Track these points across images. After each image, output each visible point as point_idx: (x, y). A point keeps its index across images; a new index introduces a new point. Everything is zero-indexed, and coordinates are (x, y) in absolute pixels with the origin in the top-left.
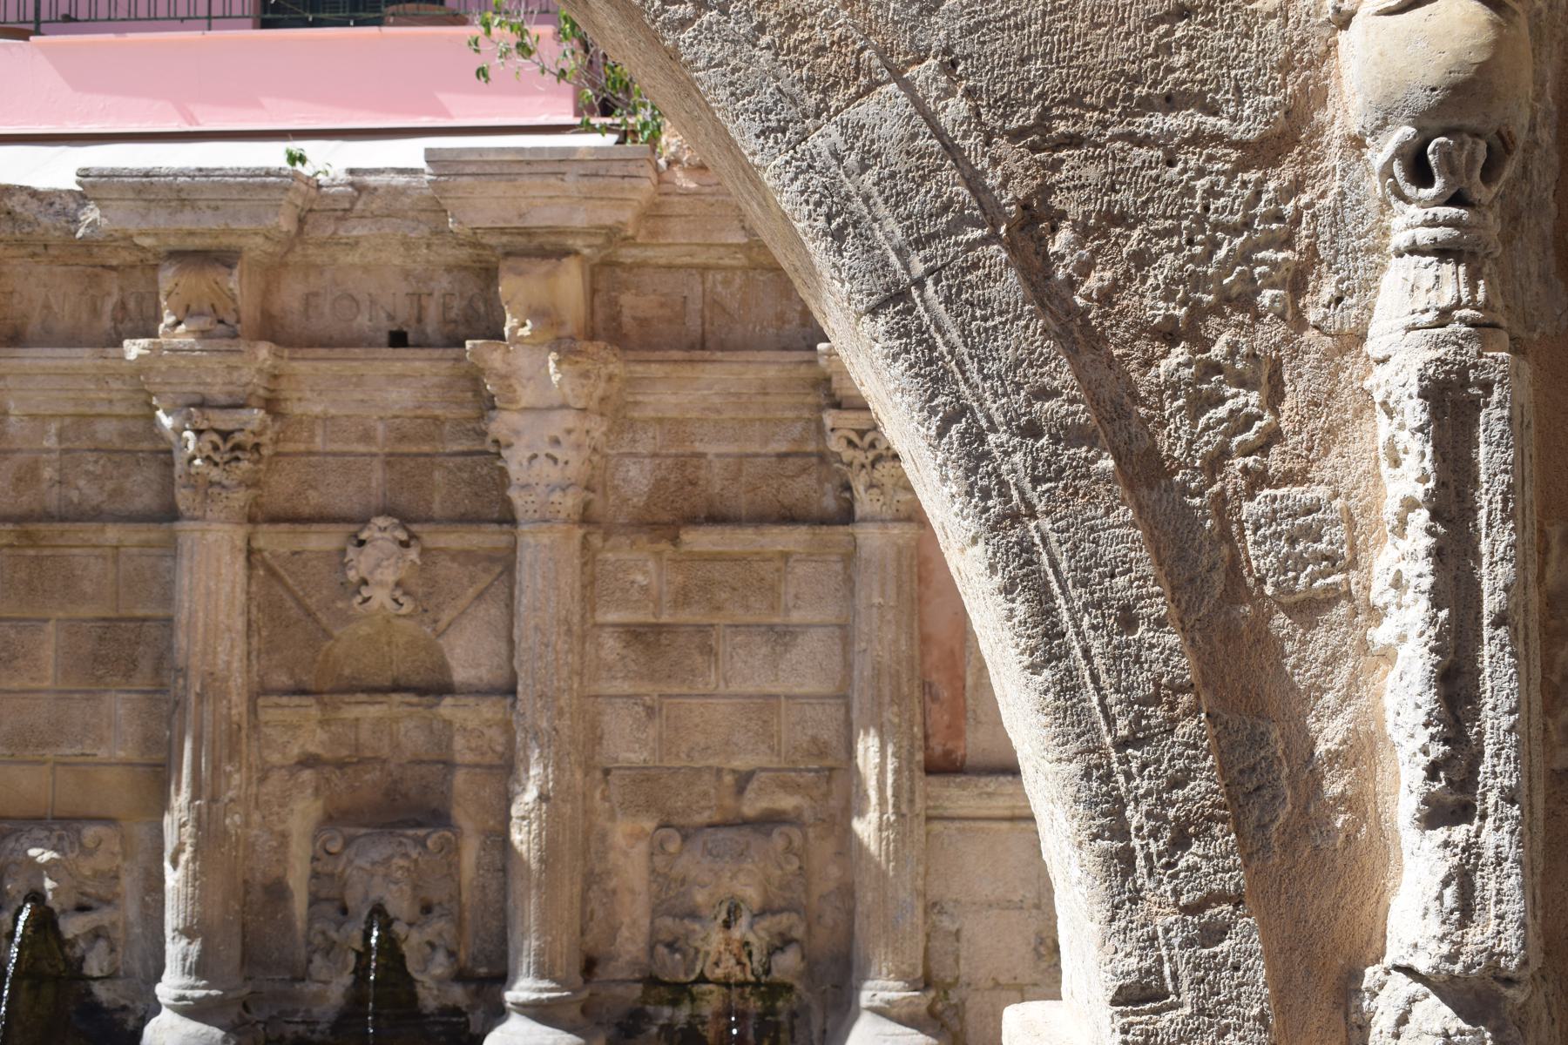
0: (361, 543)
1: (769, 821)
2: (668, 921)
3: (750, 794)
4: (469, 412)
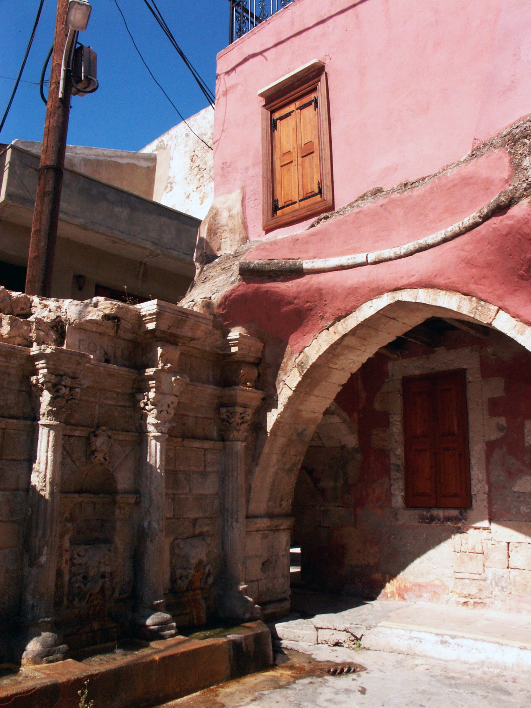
0: (96, 436)
1: (201, 535)
2: (181, 570)
3: (197, 527)
4: (130, 391)
